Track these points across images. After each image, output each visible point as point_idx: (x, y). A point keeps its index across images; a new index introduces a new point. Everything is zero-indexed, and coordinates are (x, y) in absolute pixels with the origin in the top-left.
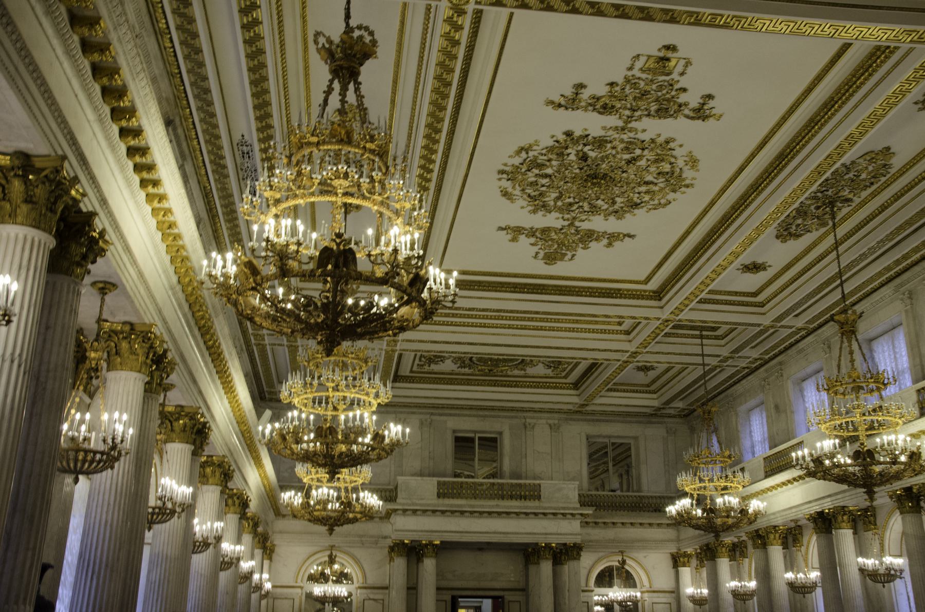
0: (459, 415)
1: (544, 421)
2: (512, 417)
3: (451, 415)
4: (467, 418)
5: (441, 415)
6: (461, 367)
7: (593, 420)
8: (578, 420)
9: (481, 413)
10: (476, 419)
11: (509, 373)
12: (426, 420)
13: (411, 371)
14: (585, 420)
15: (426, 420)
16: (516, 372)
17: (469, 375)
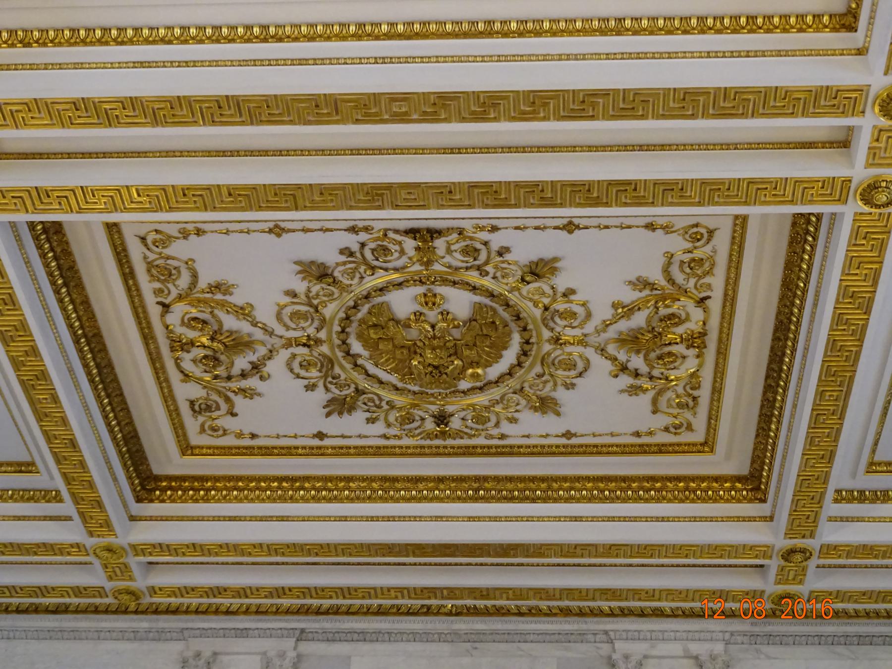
0: (389, 637)
1: (676, 648)
2: (567, 638)
3: (363, 637)
4: (412, 647)
5: (332, 638)
6: (339, 406)
7: (846, 640)
8: (796, 640)
9: (462, 625)
10: (446, 648)
11: (515, 433)
12: (282, 655)
13: (187, 449)
14: (820, 640)
15: (282, 655)
16: (532, 426)
17: (378, 452)
